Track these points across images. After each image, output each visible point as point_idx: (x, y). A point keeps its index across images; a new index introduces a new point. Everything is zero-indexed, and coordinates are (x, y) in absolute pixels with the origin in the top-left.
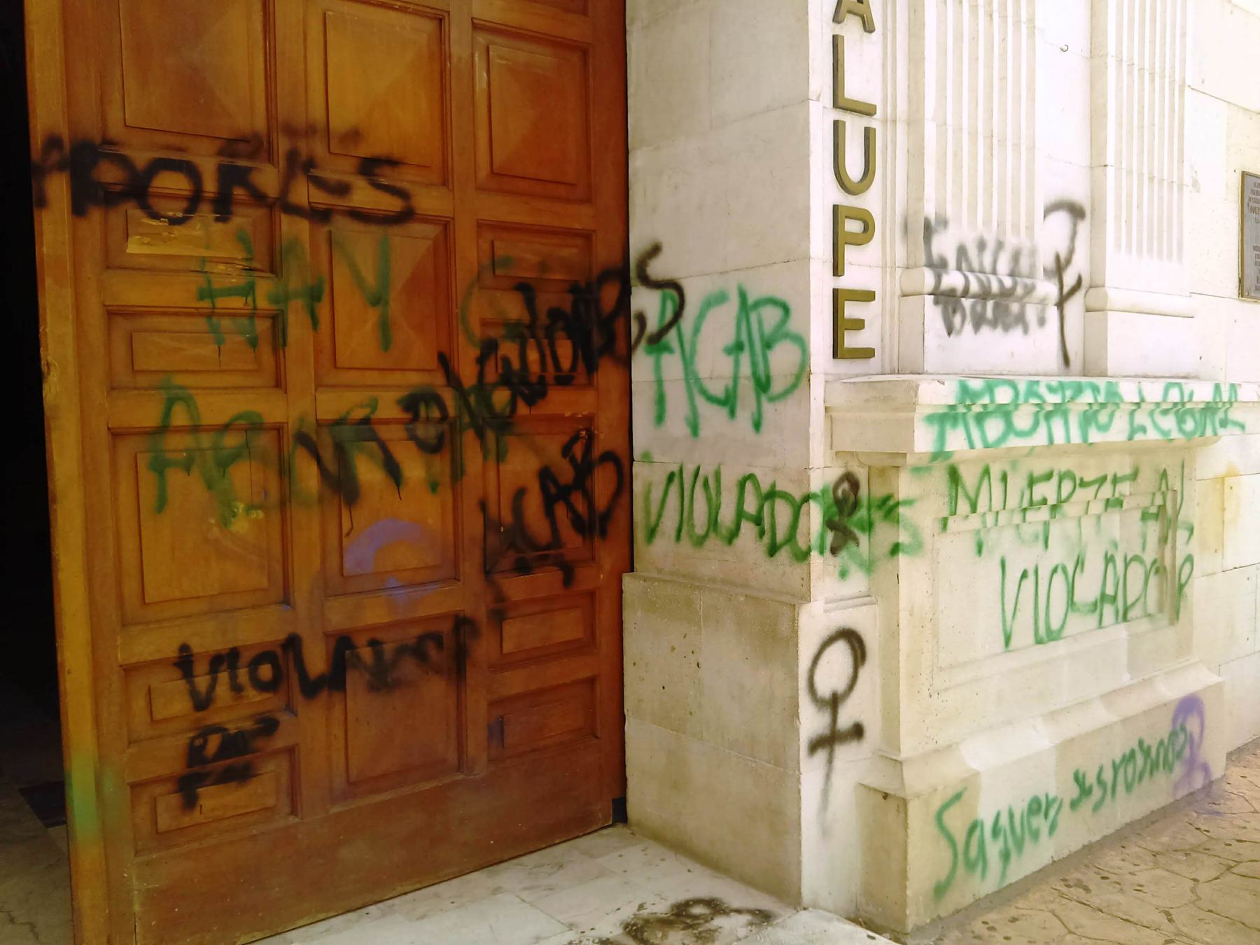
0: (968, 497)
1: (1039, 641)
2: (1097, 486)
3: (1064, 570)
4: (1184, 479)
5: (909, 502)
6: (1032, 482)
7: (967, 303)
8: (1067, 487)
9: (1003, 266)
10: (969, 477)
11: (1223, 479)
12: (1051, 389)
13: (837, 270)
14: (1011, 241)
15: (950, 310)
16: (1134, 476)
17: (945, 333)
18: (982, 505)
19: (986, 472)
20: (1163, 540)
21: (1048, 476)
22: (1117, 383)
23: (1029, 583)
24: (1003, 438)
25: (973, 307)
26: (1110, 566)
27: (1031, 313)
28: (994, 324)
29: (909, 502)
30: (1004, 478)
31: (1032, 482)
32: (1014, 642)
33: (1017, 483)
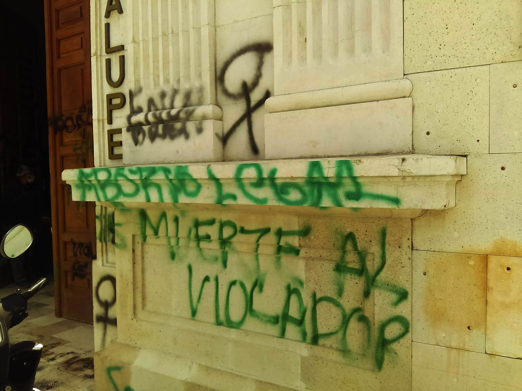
0: (152, 227)
1: (219, 323)
2: (258, 235)
3: (242, 285)
4: (387, 247)
5: (120, 225)
6: (197, 224)
7: (146, 128)
8: (227, 232)
9: (178, 103)
10: (153, 216)
11: (485, 258)
12: (132, 172)
13: (110, 122)
14: (184, 86)
15: (136, 132)
16: (305, 232)
17: (133, 144)
18: (162, 231)
19: (164, 215)
20: (367, 294)
21: (211, 222)
22: (186, 167)
23: (210, 286)
24: (117, 196)
25: (150, 129)
26: (294, 299)
27: (191, 127)
28: (163, 137)
29: (120, 225)
30: (176, 220)
31: (197, 224)
32: (198, 315)
33: (185, 224)
